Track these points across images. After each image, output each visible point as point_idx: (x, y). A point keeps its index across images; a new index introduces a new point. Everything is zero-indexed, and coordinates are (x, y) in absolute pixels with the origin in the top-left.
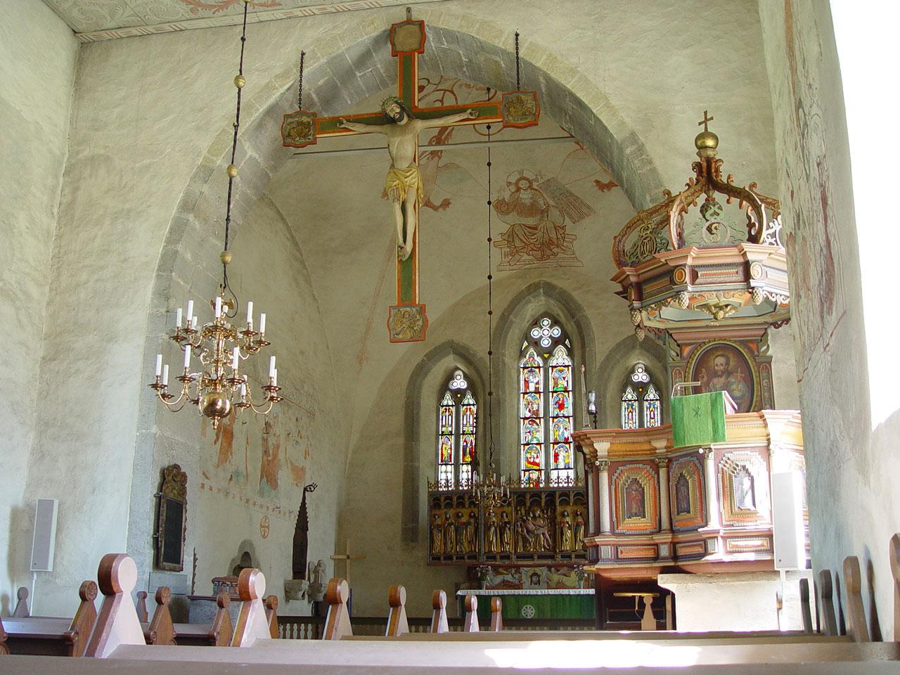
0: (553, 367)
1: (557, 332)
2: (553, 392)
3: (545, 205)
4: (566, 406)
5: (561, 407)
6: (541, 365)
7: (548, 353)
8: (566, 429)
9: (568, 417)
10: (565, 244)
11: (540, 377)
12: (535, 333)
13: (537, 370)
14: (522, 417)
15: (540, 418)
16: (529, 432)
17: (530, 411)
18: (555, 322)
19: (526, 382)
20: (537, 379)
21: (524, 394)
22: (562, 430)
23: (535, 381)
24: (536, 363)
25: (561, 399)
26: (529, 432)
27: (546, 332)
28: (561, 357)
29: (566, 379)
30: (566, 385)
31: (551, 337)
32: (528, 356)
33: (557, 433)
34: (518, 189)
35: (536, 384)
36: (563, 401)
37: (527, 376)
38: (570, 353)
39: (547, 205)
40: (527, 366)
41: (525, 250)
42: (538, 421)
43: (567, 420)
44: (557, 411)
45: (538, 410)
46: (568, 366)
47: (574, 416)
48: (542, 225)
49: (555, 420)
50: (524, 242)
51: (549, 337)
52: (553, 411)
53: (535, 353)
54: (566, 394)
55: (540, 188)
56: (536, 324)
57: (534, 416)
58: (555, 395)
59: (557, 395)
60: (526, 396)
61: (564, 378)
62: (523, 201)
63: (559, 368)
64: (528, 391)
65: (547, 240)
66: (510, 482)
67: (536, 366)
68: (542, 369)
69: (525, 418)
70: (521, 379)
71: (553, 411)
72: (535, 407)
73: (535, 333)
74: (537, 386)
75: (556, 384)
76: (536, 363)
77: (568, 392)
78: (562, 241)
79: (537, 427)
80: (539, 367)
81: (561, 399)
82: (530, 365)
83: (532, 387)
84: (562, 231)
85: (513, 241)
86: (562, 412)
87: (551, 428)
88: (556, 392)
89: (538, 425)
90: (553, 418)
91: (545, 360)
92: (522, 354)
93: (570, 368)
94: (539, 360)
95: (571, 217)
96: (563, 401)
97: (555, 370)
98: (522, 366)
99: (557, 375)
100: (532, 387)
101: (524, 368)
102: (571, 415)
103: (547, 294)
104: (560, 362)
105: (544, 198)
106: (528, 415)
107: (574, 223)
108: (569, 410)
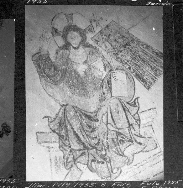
3: (105, 70)
10: (142, 132)
34: (67, 46)
39: (108, 70)
41: (84, 159)
48: (103, 110)
50: (83, 144)
55: (97, 41)
62: (75, 67)
65: (115, 136)
78: (136, 127)
84: (134, 110)
85: (67, 135)
95: (144, 81)
105: (103, 58)
107: (149, 88)
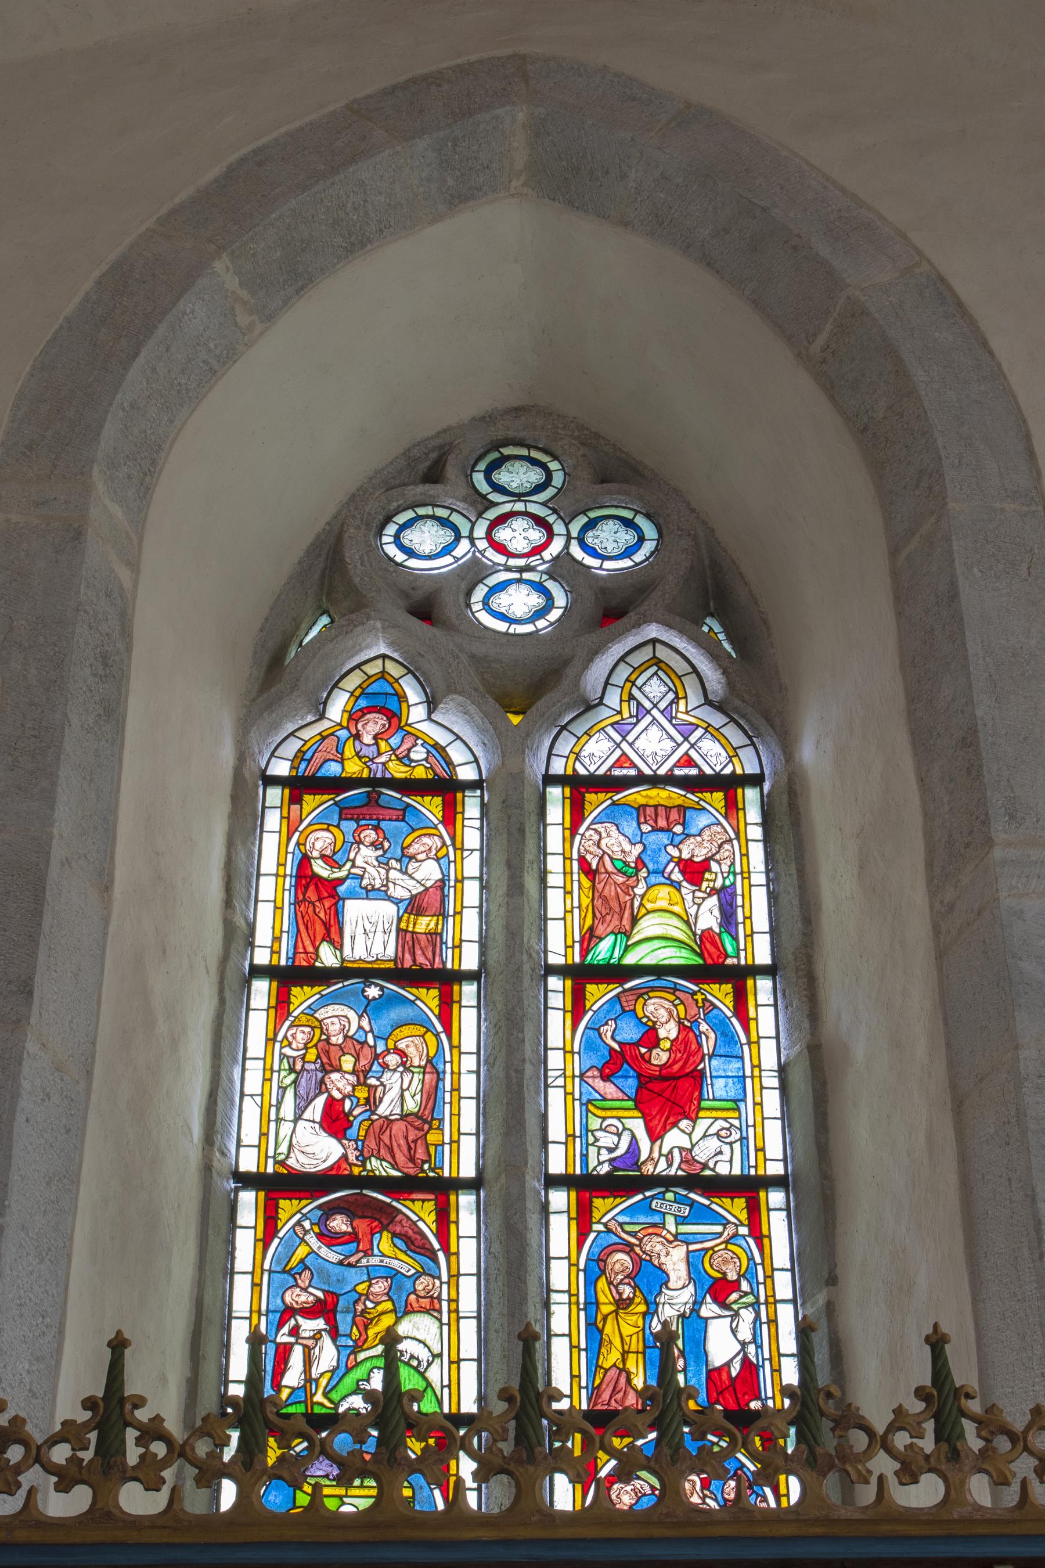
0: (580, 787)
1: (614, 547)
2: (581, 975)
4: (718, 1088)
5: (669, 1092)
6: (466, 773)
7: (530, 687)
8: (720, 1290)
9: (748, 1187)
11: (452, 857)
12: (425, 546)
13: (431, 808)
14: (248, 1163)
15: (442, 1190)
16: (323, 1308)
17: (335, 1122)
18: (606, 471)
19: (318, 896)
20: (429, 872)
21: (288, 978)
22: (677, 1298)
23: (403, 888)
24: (419, 754)
25: (669, 1031)
26: (323, 1308)
27: (519, 536)
28: (653, 721)
29: (717, 876)
30: (709, 918)
31: (564, 568)
32: (337, 708)
33: (630, 1324)
35: (415, 906)
36: (686, 1043)
37: (321, 841)
38: (755, 697)
40: (333, 769)
42: (421, 1213)
43: (736, 1208)
44: (621, 1133)
45: (424, 1120)
46: (729, 785)
47: (818, 1188)
49: (608, 1210)
51: (551, 575)
52: (579, 1123)
53: (413, 694)
54: (721, 995)
56: (434, 475)
57: (379, 1167)
58: (599, 995)
59: (623, 1007)
60: (302, 997)
61: (695, 871)
63: (636, 795)
64: (328, 957)
66: (110, 1450)
67: (420, 773)
68: (471, 807)
69: (280, 1185)
70: (269, 863)
71: (579, 1123)
72: (398, 1093)
73: (425, 546)
74: (424, 924)
75: (612, 905)
76: (419, 754)
77: (739, 977)
79: (405, 1264)
80: (446, 788)
81: (669, 1031)
82: (353, 768)
83: (369, 930)
86: (674, 1138)
87: (559, 1275)
88: (614, 973)
89: (414, 1243)
90: (587, 1187)
91: (510, 747)
92: (276, 678)
93: (751, 795)
94: (451, 736)
96: (686, 1043)
97: (597, 803)
98: (281, 768)
99: (615, 841)
100: (369, 930)
101: (299, 787)
102: (775, 1169)
103: (567, 180)
104: (654, 746)
106: (318, 1151)
108: (745, 1123)
